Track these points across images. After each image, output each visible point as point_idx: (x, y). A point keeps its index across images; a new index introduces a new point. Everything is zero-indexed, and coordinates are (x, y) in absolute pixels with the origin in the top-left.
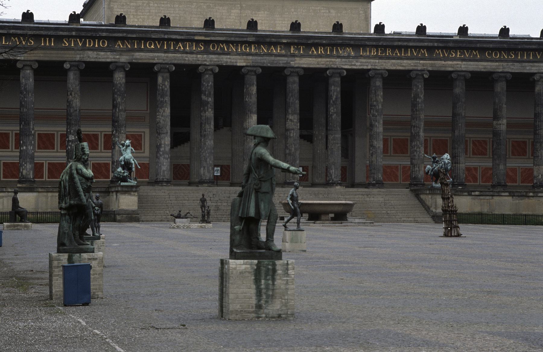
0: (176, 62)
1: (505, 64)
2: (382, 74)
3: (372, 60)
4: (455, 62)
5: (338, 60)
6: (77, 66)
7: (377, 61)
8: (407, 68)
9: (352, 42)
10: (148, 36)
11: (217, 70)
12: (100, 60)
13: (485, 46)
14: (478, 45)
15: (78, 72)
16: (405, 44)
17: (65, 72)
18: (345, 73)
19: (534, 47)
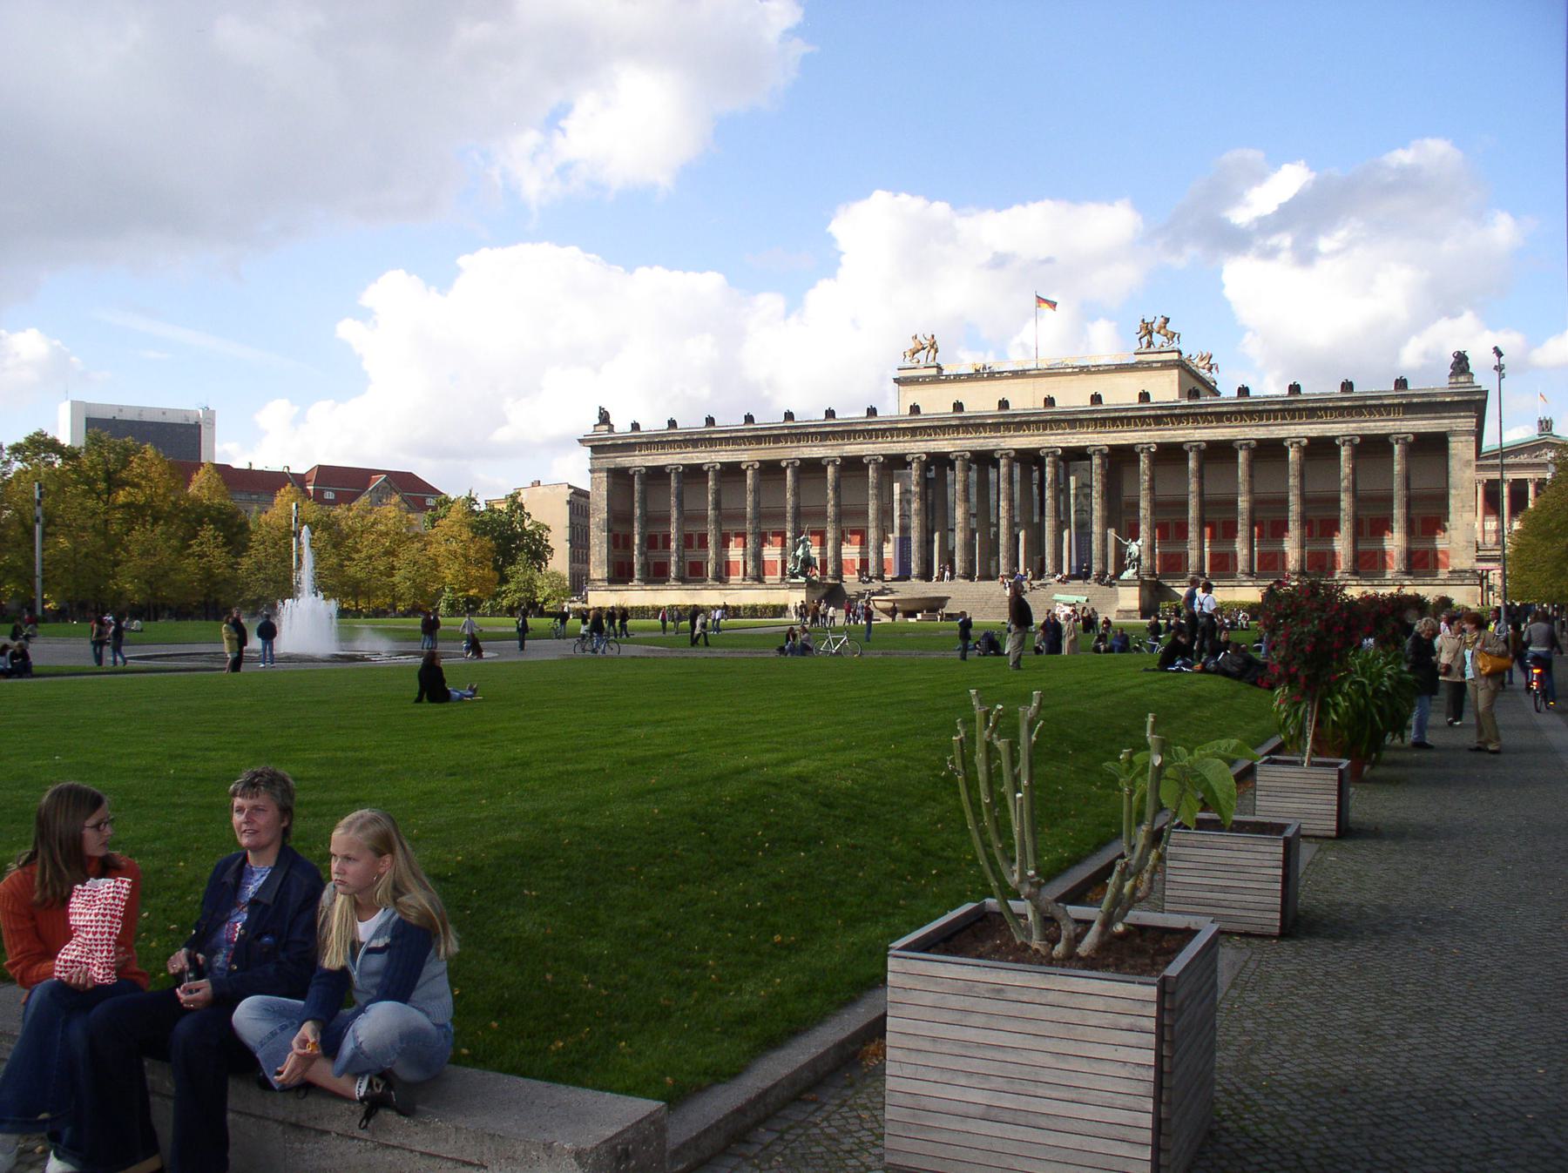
0: (884, 453)
1: (1246, 429)
2: (1100, 450)
3: (1090, 436)
4: (1187, 431)
5: (1053, 437)
6: (793, 463)
7: (1096, 436)
8: (1131, 442)
9: (1063, 417)
10: (853, 428)
11: (924, 457)
12: (814, 456)
13: (1218, 409)
14: (1209, 410)
16: (1123, 414)
17: (784, 470)
18: (1060, 451)
19: (1277, 407)
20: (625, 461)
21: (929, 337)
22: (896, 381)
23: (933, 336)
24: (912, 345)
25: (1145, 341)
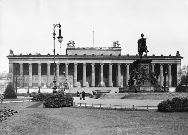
11: (86, 64)
15: (59, 65)
20: (17, 62)
21: (73, 41)
23: (74, 41)
24: (69, 42)
25: (114, 45)
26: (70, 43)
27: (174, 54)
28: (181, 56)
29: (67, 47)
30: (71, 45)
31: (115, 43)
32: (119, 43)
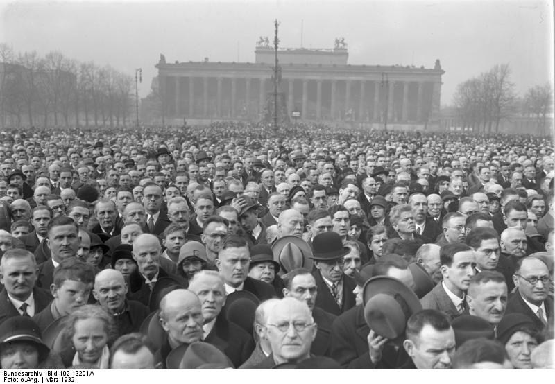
22: (256, 52)
24: (259, 40)
26: (262, 41)
27: (430, 65)
28: (442, 68)
29: (257, 48)
30: (263, 44)
31: (337, 42)
32: (345, 41)
